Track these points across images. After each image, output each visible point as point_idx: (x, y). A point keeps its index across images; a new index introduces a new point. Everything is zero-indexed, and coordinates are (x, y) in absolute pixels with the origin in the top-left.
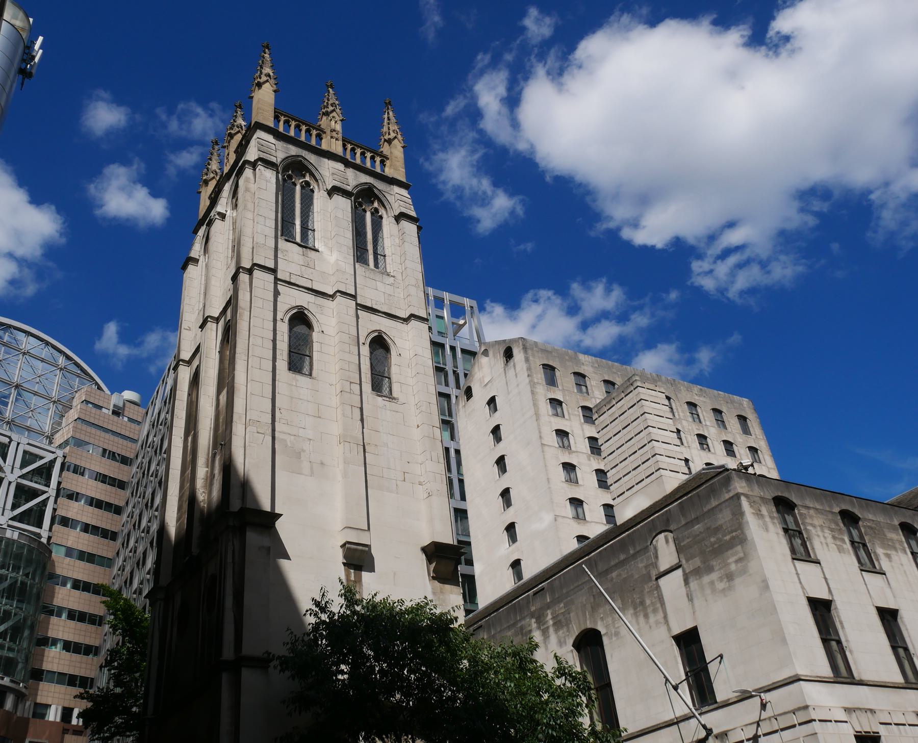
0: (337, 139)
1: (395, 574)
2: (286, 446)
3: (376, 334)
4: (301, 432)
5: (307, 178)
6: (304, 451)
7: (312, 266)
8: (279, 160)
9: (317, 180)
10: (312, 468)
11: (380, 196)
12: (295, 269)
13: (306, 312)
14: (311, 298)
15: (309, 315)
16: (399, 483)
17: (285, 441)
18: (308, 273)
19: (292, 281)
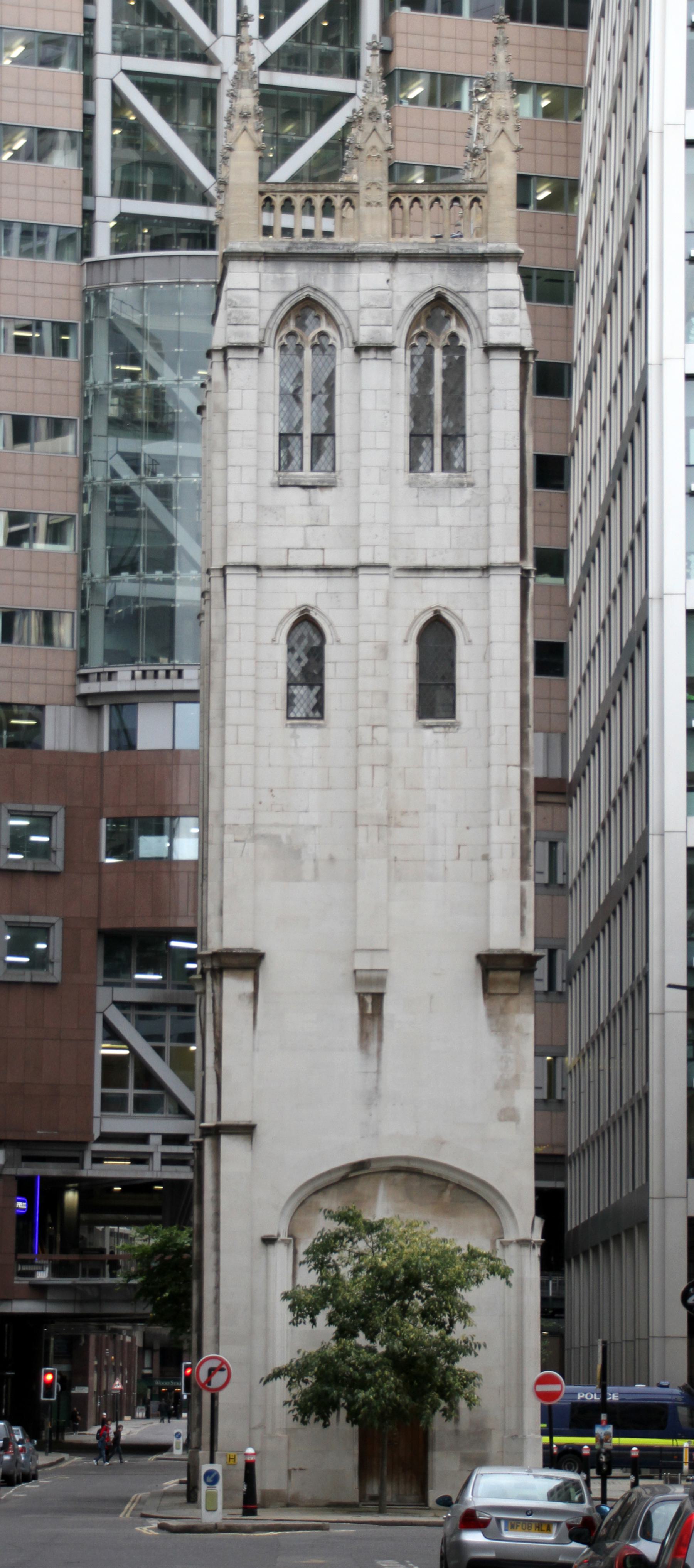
1: (432, 997)
3: (430, 615)
9: (337, 327)
10: (316, 870)
11: (460, 307)
12: (294, 538)
19: (292, 562)
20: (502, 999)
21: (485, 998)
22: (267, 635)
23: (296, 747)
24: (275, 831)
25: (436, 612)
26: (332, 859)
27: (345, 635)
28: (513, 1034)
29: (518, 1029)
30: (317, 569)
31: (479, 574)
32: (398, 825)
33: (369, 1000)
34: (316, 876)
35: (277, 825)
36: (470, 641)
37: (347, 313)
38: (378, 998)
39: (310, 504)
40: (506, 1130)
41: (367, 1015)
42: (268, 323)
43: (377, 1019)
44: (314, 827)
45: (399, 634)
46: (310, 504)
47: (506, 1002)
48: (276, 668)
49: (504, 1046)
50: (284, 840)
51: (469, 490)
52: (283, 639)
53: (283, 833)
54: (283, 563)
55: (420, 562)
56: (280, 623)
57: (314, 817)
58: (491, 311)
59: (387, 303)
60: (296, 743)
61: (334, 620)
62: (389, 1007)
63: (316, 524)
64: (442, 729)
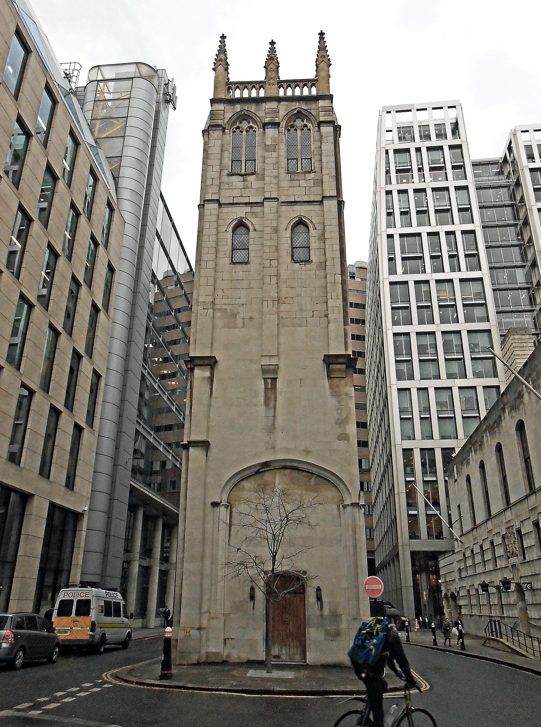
1: (301, 379)
2: (226, 312)
3: (297, 219)
7: (249, 186)
8: (226, 120)
10: (244, 323)
11: (307, 114)
12: (237, 193)
16: (308, 319)
24: (224, 307)
26: (251, 318)
28: (344, 397)
29: (346, 394)
30: (246, 203)
33: (269, 381)
34: (244, 326)
35: (225, 304)
43: (273, 390)
44: (243, 305)
50: (229, 311)
52: (230, 230)
53: (228, 308)
57: (243, 301)
62: (279, 384)
63: (246, 188)
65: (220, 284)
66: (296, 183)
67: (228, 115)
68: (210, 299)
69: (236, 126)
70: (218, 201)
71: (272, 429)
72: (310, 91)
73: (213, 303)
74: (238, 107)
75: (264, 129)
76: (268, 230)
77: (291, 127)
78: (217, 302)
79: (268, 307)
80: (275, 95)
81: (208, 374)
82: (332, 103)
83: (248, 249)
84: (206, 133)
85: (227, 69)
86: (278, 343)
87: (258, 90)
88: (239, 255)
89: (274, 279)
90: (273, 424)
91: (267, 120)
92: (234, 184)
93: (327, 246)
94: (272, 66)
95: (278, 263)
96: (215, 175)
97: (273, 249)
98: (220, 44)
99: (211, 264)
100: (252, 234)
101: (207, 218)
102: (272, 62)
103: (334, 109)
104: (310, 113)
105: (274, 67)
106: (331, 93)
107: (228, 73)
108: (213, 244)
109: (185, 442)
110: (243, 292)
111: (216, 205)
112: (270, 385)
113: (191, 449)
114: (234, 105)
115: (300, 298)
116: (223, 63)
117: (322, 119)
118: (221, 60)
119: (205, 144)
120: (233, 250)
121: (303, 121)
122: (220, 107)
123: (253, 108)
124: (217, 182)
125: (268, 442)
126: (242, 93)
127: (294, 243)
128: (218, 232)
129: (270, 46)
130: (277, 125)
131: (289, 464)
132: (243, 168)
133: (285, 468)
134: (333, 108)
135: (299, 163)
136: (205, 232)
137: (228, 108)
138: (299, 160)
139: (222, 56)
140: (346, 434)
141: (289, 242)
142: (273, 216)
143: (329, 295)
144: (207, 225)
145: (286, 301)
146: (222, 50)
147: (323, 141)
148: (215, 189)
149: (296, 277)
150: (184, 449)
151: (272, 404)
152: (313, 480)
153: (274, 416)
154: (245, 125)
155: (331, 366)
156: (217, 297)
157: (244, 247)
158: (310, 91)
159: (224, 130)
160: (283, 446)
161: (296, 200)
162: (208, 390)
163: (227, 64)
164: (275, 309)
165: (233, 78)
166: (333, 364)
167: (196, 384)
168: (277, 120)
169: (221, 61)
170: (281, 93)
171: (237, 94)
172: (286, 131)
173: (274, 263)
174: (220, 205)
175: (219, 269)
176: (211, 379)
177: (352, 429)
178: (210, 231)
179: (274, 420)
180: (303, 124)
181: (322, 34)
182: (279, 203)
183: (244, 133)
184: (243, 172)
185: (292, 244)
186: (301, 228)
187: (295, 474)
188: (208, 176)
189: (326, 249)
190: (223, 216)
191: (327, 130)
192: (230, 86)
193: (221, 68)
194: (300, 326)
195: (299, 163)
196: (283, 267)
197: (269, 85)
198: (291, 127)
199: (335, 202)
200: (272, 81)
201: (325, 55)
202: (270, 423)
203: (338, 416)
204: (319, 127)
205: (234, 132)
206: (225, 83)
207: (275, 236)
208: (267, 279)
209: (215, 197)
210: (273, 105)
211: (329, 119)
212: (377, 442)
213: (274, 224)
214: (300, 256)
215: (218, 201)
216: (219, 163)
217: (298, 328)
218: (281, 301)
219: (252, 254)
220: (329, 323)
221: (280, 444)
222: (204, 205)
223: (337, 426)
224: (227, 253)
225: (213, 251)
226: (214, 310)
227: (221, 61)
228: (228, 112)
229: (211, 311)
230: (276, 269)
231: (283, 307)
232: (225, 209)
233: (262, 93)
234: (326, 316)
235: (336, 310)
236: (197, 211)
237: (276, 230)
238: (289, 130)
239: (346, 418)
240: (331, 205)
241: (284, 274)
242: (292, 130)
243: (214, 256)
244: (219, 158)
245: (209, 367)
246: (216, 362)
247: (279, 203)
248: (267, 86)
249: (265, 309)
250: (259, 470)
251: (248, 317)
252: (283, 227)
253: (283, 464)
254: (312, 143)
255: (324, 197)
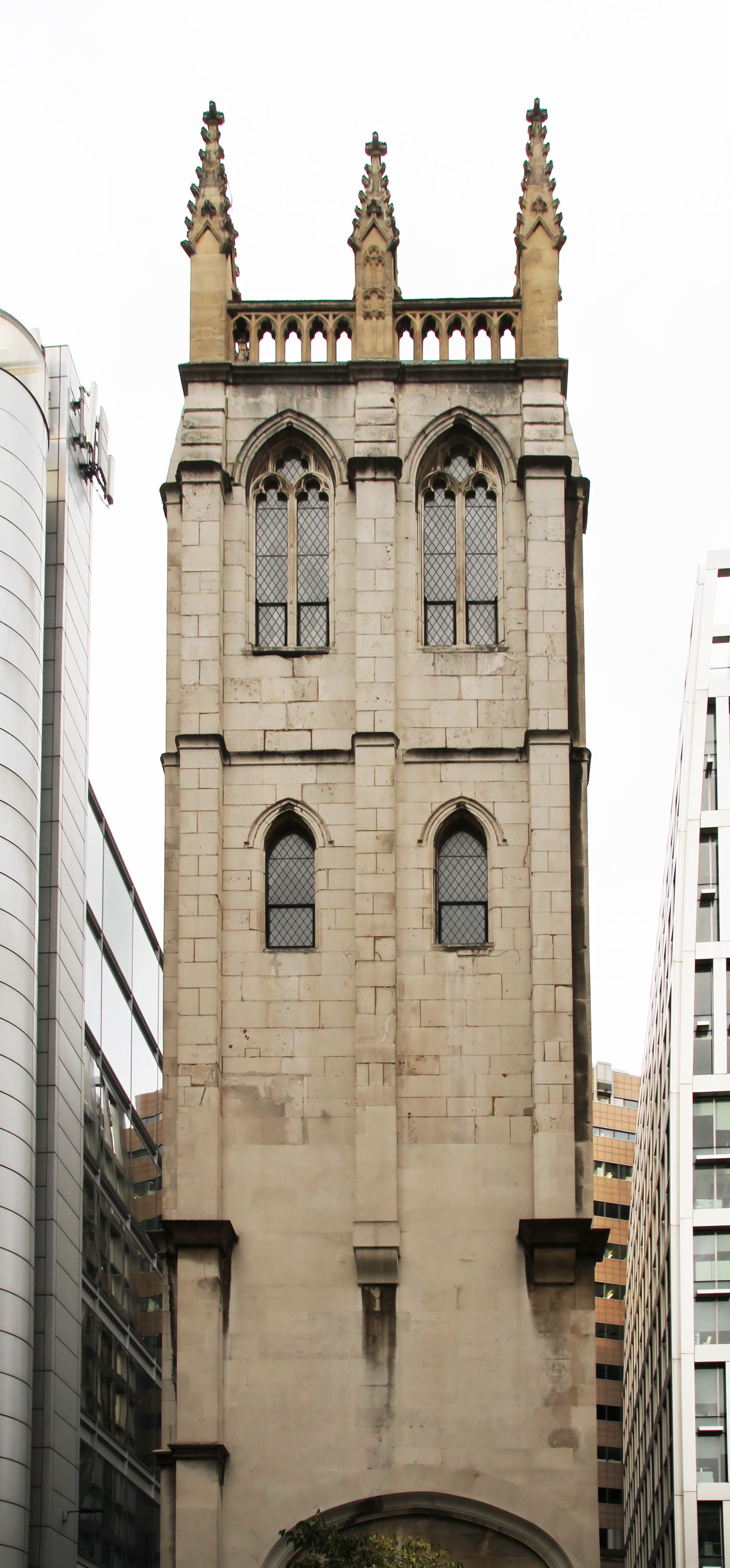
0: (380, 316)
1: (459, 1290)
2: (257, 1097)
3: (452, 809)
4: (286, 1066)
5: (312, 470)
6: (290, 1099)
10: (304, 1130)
11: (488, 436)
12: (274, 717)
13: (297, 810)
14: (308, 773)
15: (305, 816)
16: (480, 1121)
17: (255, 1089)
18: (303, 715)
19: (270, 748)
20: (552, 1291)
21: (530, 1291)
22: (236, 837)
23: (277, 976)
24: (251, 1082)
25: (459, 805)
26: (325, 1116)
27: (339, 836)
28: (568, 1336)
29: (575, 1330)
30: (302, 754)
31: (516, 757)
32: (412, 1073)
33: (376, 1293)
34: (305, 1137)
35: (252, 1074)
36: (504, 840)
37: (340, 443)
38: (389, 1291)
39: (294, 676)
40: (559, 1459)
41: (374, 1312)
42: (238, 456)
43: (387, 1319)
44: (301, 1076)
45: (409, 834)
46: (294, 676)
47: (558, 1294)
48: (250, 878)
49: (556, 1351)
50: (263, 1094)
51: (502, 654)
52: (259, 842)
53: (261, 1084)
54: (261, 749)
55: (439, 744)
56: (256, 822)
57: (302, 1064)
58: (527, 428)
59: (391, 421)
60: (277, 972)
61: (327, 816)
63: (301, 701)
64: (469, 952)
65: (236, 1016)
66: (448, 687)
67: (241, 431)
68: (208, 1056)
69: (263, 476)
70: (218, 739)
71: (382, 1417)
72: (496, 348)
73: (219, 1067)
74: (270, 401)
75: (352, 488)
76: (367, 842)
77: (434, 484)
78: (231, 1066)
79: (370, 1082)
80: (386, 357)
81: (212, 1271)
82: (564, 392)
83: (312, 906)
84: (172, 498)
85: (228, 250)
86: (399, 1190)
87: (331, 336)
88: (287, 918)
89: (386, 997)
90: (388, 1406)
91: (361, 451)
92: (265, 683)
93: (536, 897)
94: (374, 239)
95: (398, 950)
96: (208, 649)
97: (382, 902)
98: (203, 146)
99: (208, 950)
100: (323, 856)
101: (188, 801)
102: (375, 227)
103: (571, 419)
104: (496, 430)
105: (383, 247)
106: (562, 355)
107: (235, 273)
108: (210, 886)
109: (165, 1449)
110: (303, 1038)
111: (214, 756)
112: (378, 1302)
113: (180, 1467)
114: (257, 395)
115: (457, 1058)
116: (216, 222)
117: (531, 450)
118: (208, 209)
119: (173, 536)
120: (269, 908)
121: (472, 463)
122: (211, 395)
123: (314, 404)
124: (211, 675)
125: (373, 1451)
126: (281, 349)
127: (442, 890)
128: (223, 847)
129: (368, 160)
130: (391, 466)
131: (426, 1504)
132: (291, 625)
133: (417, 1514)
134: (565, 414)
135: (461, 616)
136: (185, 845)
137: (239, 401)
138: (461, 605)
139: (212, 195)
140: (570, 1431)
141: (429, 883)
142: (381, 796)
143: (538, 1047)
144: (189, 823)
145: (420, 1066)
146: (212, 170)
147: (531, 535)
148: (210, 702)
149: (447, 997)
150: (163, 1466)
151: (383, 1354)
152: (486, 1544)
153: (390, 1385)
154: (293, 473)
155: (538, 1253)
156: (228, 1052)
157: (299, 900)
158: (496, 348)
159: (227, 485)
160: (411, 1461)
161: (451, 745)
162: (217, 1317)
163: (228, 226)
164: (389, 1088)
165: (252, 290)
166: (543, 1246)
167: (183, 1295)
168: (390, 450)
169: (211, 222)
170: (406, 351)
171: (266, 351)
172: (421, 499)
173: (386, 947)
174: (226, 755)
175: (232, 966)
176: (224, 1284)
177: (584, 1420)
178: (200, 844)
179: (389, 1396)
180: (472, 472)
181: (537, 115)
182: (400, 753)
183: (292, 501)
184: (292, 646)
185: (437, 891)
186: (462, 843)
187: (443, 1530)
188: (186, 655)
189: (535, 909)
190: (236, 794)
191: (547, 492)
192: (244, 319)
193: (208, 245)
194: (458, 1139)
195: (461, 616)
196: (411, 965)
197: (367, 316)
198: (434, 484)
199: (560, 754)
200: (375, 304)
201: (546, 199)
202: (379, 1402)
203: (550, 1386)
204: (521, 484)
205: (261, 498)
206: (223, 304)
207: (386, 861)
208: (366, 997)
209: (209, 727)
210: (378, 393)
211: (555, 450)
212: (647, 1466)
213: (385, 822)
214: (460, 922)
215: (218, 739)
216: (216, 608)
217: (452, 1146)
218: (405, 1068)
219: (324, 921)
220: (534, 1130)
221: (405, 1456)
222: (177, 755)
223: (549, 1410)
224: (254, 915)
225: (209, 906)
226: (223, 1091)
227: (211, 222)
228: (239, 418)
229: (213, 1092)
230: (388, 968)
231: (413, 1085)
232: (243, 774)
233: (345, 351)
234: (529, 1113)
235: (556, 1092)
236: (158, 776)
237: (391, 842)
238: (429, 497)
239: (574, 1390)
240: (551, 759)
241: (416, 982)
242: (439, 496)
243: (214, 922)
244: (216, 586)
245: (215, 1253)
246: (233, 1239)
247: (400, 753)
248: (359, 319)
249: (362, 1087)
250: (353, 1519)
251: (319, 1114)
252: (409, 834)
253: (413, 1504)
254: (500, 545)
255: (530, 734)
